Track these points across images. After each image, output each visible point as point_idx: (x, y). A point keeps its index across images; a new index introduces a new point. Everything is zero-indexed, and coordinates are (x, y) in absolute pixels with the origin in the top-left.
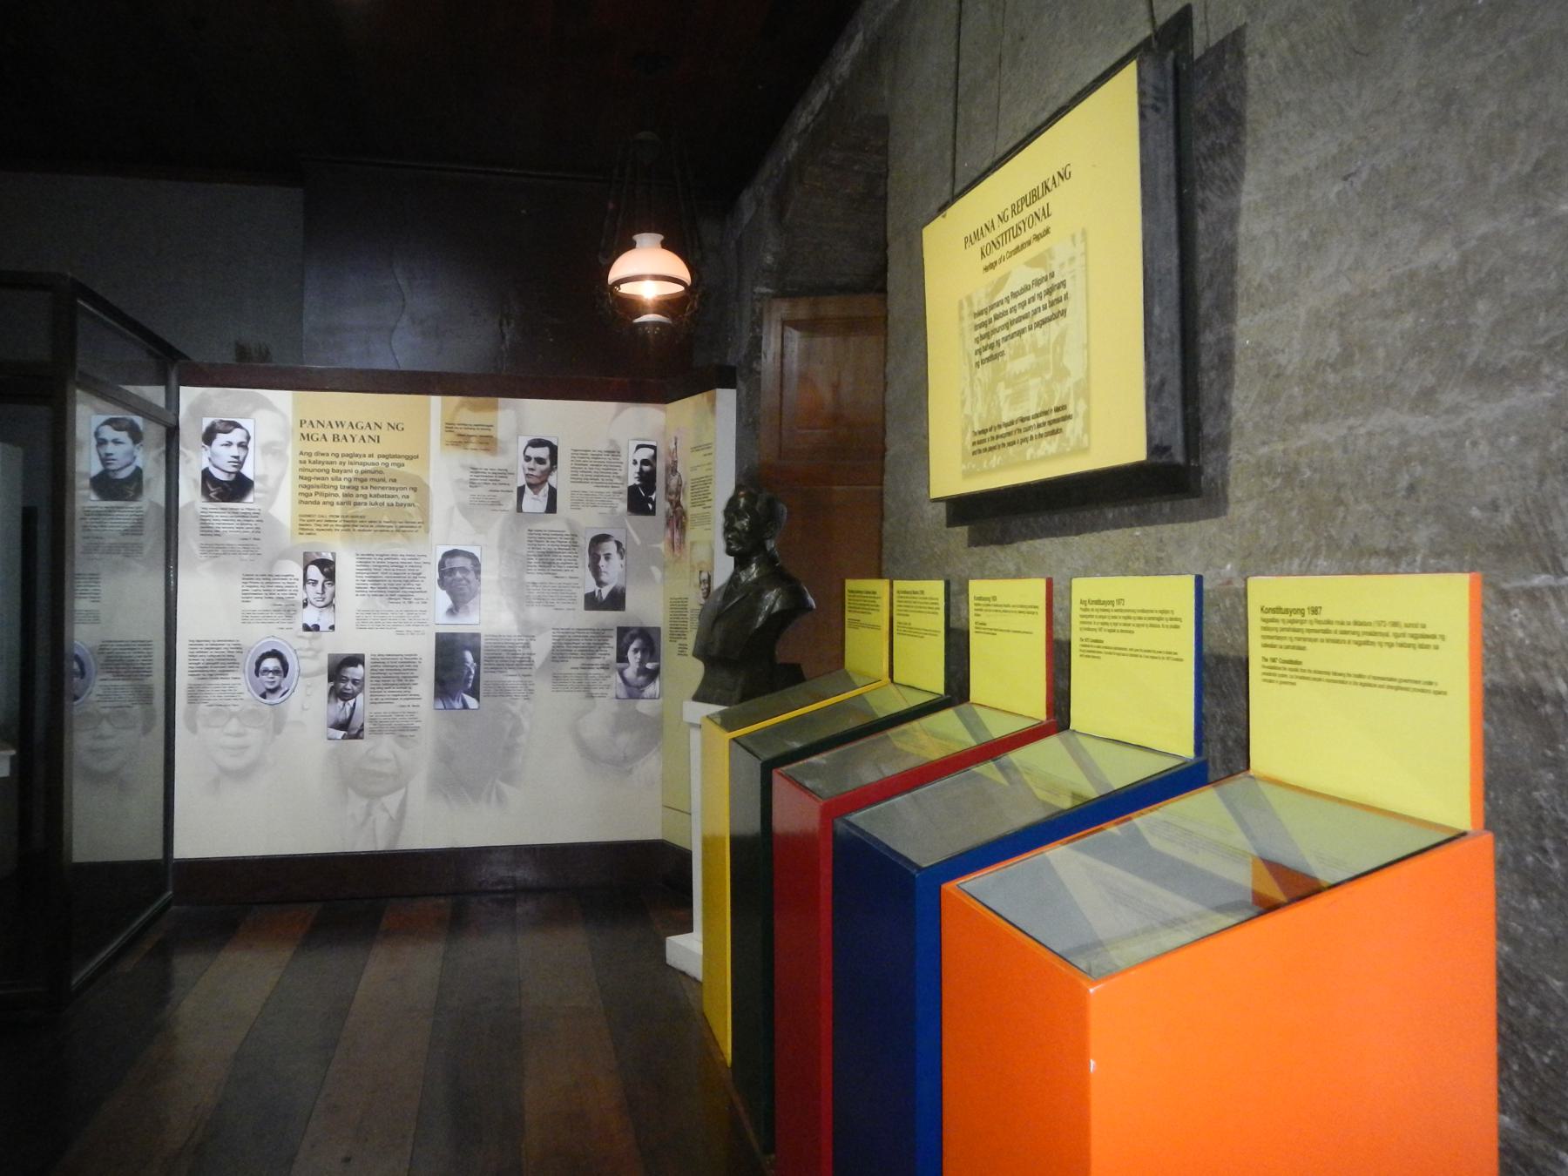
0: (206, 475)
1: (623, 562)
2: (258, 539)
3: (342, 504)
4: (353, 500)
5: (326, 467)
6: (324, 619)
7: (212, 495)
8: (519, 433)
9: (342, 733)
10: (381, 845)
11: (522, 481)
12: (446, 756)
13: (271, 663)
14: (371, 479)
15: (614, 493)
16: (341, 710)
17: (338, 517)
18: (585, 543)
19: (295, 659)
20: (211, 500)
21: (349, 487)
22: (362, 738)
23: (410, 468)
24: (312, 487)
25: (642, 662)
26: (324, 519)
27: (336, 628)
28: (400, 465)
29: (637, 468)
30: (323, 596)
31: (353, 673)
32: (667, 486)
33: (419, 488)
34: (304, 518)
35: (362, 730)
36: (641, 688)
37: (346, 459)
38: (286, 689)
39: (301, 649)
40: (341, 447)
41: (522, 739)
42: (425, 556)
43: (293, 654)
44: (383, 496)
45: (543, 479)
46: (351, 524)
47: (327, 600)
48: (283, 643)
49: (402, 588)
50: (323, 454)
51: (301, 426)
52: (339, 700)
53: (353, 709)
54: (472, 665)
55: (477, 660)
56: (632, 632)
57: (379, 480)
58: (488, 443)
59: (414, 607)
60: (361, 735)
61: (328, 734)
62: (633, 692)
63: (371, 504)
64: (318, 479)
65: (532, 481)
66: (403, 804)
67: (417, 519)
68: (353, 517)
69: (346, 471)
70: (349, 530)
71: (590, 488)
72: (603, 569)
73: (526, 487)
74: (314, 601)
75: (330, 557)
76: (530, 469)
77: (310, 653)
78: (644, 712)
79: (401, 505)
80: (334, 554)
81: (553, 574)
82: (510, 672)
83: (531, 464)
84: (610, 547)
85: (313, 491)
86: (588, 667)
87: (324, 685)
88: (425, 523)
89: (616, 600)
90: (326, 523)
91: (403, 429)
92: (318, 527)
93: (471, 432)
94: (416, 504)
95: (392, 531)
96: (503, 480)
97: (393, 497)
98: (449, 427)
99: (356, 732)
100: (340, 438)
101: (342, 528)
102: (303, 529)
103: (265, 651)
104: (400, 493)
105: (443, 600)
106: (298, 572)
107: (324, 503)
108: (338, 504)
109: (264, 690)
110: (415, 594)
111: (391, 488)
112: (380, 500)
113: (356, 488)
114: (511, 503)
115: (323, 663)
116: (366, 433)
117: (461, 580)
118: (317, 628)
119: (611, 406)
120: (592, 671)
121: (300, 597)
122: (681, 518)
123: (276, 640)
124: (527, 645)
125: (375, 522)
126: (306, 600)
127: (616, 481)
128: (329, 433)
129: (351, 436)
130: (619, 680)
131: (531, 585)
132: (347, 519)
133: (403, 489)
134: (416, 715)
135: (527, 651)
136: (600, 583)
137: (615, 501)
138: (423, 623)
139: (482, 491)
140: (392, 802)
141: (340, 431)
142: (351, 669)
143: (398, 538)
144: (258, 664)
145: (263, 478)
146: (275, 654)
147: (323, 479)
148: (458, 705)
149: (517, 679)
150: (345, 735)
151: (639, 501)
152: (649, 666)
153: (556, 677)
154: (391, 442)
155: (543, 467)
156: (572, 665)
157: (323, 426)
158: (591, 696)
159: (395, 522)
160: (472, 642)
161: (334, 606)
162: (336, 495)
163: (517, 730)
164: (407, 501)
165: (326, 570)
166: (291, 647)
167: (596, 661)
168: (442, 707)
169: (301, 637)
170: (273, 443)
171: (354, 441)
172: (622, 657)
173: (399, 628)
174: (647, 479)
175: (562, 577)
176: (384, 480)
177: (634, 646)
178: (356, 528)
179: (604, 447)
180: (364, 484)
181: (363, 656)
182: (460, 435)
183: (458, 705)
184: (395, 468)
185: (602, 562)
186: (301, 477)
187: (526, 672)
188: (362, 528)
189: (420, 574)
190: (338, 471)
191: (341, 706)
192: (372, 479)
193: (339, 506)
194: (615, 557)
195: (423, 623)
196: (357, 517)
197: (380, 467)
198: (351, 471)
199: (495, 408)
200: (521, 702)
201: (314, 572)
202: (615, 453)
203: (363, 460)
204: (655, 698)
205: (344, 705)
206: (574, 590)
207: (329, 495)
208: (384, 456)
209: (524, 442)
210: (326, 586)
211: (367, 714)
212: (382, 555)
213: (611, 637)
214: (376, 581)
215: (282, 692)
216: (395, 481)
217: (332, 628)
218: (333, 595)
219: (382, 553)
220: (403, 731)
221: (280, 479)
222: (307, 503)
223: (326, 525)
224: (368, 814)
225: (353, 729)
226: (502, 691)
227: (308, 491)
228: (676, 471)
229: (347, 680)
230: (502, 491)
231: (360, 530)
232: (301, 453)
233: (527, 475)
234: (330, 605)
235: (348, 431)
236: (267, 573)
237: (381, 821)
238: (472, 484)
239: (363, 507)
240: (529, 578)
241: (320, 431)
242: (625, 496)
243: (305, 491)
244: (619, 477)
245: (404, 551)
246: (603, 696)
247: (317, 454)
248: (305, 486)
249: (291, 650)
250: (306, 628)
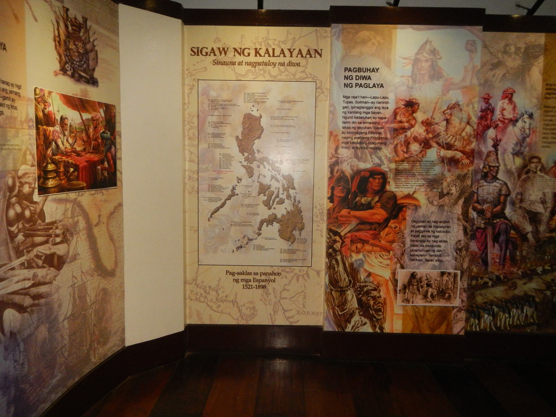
122: (507, 232)
228: (495, 178)
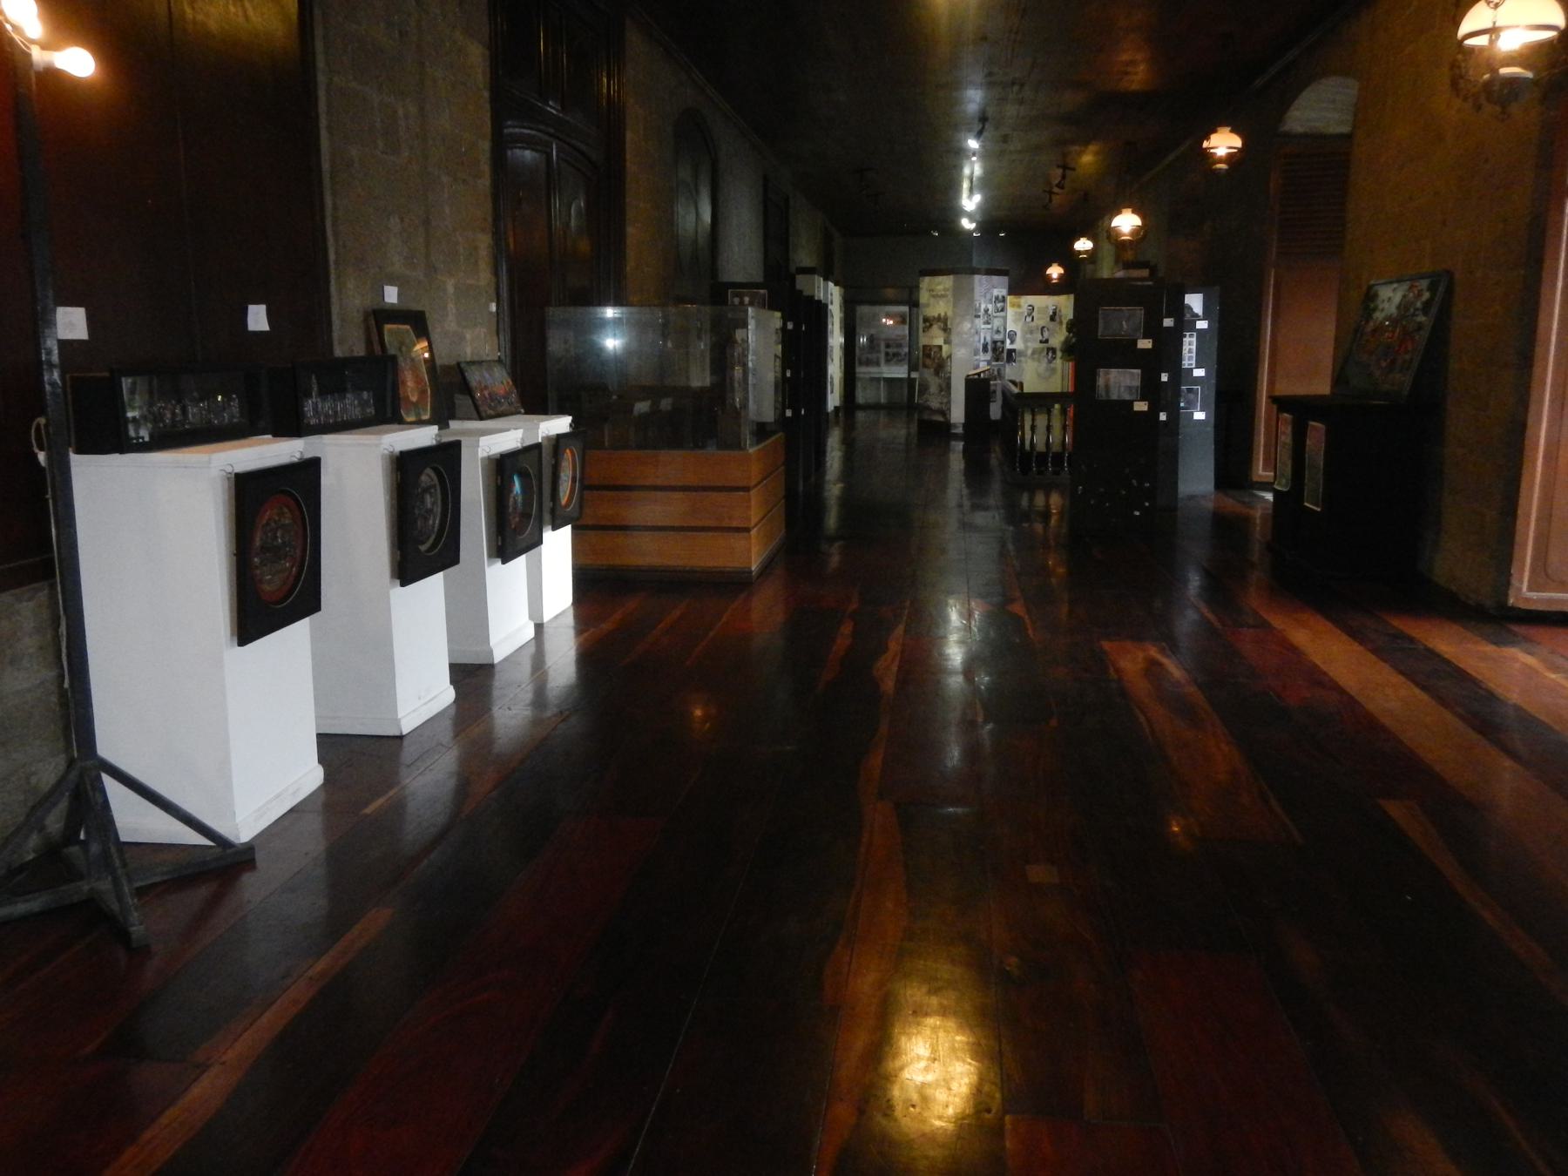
58: (1019, 306)
62: (1050, 362)
84: (1045, 329)
89: (1047, 341)
119: (1046, 297)
151: (1052, 318)
156: (1036, 356)
160: (1014, 350)
172: (1047, 354)
174: (1055, 313)
202: (1047, 307)
226: (1020, 361)
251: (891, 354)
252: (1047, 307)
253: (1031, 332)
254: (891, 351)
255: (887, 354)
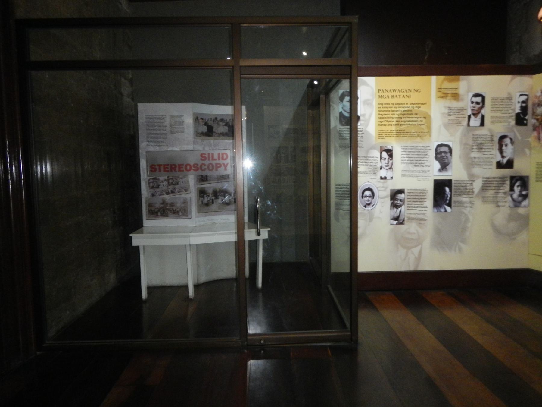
0: (341, 114)
1: (512, 147)
2: (362, 141)
3: (396, 125)
4: (400, 123)
5: (389, 109)
6: (388, 174)
7: (343, 123)
8: (469, 91)
9: (396, 222)
10: (411, 268)
11: (469, 112)
12: (438, 231)
13: (368, 193)
14: (408, 113)
15: (510, 116)
16: (395, 212)
17: (394, 131)
18: (496, 139)
19: (377, 191)
20: (343, 125)
21: (398, 118)
22: (404, 224)
23: (423, 108)
24: (383, 118)
25: (521, 191)
26: (388, 132)
27: (393, 178)
28: (419, 107)
29: (519, 105)
30: (388, 164)
31: (400, 197)
32: (534, 113)
33: (427, 117)
34: (380, 132)
35: (404, 221)
36: (520, 202)
37: (397, 106)
38: (374, 204)
39: (379, 187)
40: (395, 101)
41: (469, 225)
42: (429, 146)
43: (376, 189)
44: (412, 121)
45: (479, 111)
46: (400, 134)
47: (390, 167)
48: (373, 185)
49: (420, 161)
50: (388, 104)
51: (379, 92)
52: (395, 208)
53: (400, 212)
54: (448, 193)
55: (451, 191)
56: (516, 178)
57: (410, 114)
58: (456, 96)
59: (425, 168)
60: (403, 223)
61: (390, 222)
62: (517, 204)
63: (407, 125)
64: (386, 115)
65: (475, 112)
66: (420, 253)
67: (426, 130)
68: (400, 130)
69: (397, 111)
70: (398, 136)
71: (499, 114)
72: (504, 151)
73: (472, 116)
74: (384, 167)
75: (391, 148)
76: (474, 107)
77: (383, 189)
78: (521, 213)
79: (419, 125)
80: (392, 147)
81: (483, 153)
82: (464, 196)
83: (474, 105)
84: (507, 141)
85: (383, 120)
86: (497, 193)
87: (388, 202)
88: (429, 133)
89: (510, 164)
90: (389, 133)
91: (420, 92)
92: (386, 135)
93: (448, 92)
94: (426, 124)
95: (416, 136)
96: (462, 113)
97: (416, 121)
98: (439, 90)
99: (401, 221)
100: (395, 96)
101: (395, 135)
102: (380, 136)
103: (365, 188)
104: (419, 120)
105: (437, 165)
106: (377, 154)
107: (388, 125)
108: (394, 125)
109: (365, 204)
110: (425, 163)
111: (415, 118)
112: (411, 123)
113: (401, 118)
114: (465, 122)
115: (388, 193)
116: (405, 94)
117: (444, 156)
118: (385, 178)
119: (508, 77)
120: (499, 195)
121: (379, 165)
123: (370, 183)
124: (471, 184)
125: (409, 132)
126: (381, 166)
127: (511, 111)
128: (390, 94)
129: (399, 95)
130: (510, 199)
131: (473, 158)
132: (397, 131)
133: (421, 118)
134: (426, 215)
135: (471, 187)
136: (503, 157)
137: (510, 120)
138: (428, 175)
139: (453, 117)
140: (416, 250)
141: (394, 94)
142: (399, 195)
143: (418, 139)
144: (363, 193)
145: (364, 115)
146: (369, 189)
147: (388, 114)
148: (443, 210)
149: (467, 199)
150: (397, 223)
151: (520, 120)
152: (524, 193)
153: (484, 198)
154: (415, 98)
155: (479, 106)
156: (490, 193)
157: (387, 92)
158: (498, 206)
159: (417, 132)
160: (448, 183)
161: (392, 168)
162: (393, 121)
163: (467, 220)
164: (422, 123)
165: (389, 153)
166: (375, 186)
167: (501, 191)
168: (436, 211)
169: (379, 182)
170: (368, 100)
171: (400, 98)
172: (512, 189)
173: (419, 178)
174: (524, 109)
175: (486, 155)
176: (412, 114)
177: (517, 184)
178: (401, 135)
179: (505, 95)
180: (405, 116)
181: (404, 190)
182: (444, 93)
183: (443, 210)
184: (417, 109)
185: (504, 148)
186: (379, 114)
187: (471, 196)
188: (403, 135)
189: (427, 154)
190: (393, 111)
191: (396, 211)
192: (408, 114)
193: (394, 126)
194: (510, 145)
195: (428, 175)
196: (401, 130)
197: (411, 109)
198: (399, 111)
199: (458, 80)
200: (468, 209)
201: (385, 154)
202: (510, 98)
203: (404, 106)
204: (526, 207)
205: (397, 210)
206: (491, 160)
207: (390, 121)
208: (412, 104)
209: (471, 95)
210: (389, 160)
211: (406, 214)
212: (412, 147)
213: (507, 180)
214: (409, 157)
215: (372, 205)
216: (417, 114)
217: (392, 178)
218: (392, 164)
219: (412, 146)
220: (420, 221)
221: (370, 115)
222: (381, 125)
223: (389, 134)
224: (407, 255)
225: (401, 220)
226: (461, 204)
227: (382, 119)
229: (398, 200)
230: (461, 117)
231: (403, 136)
232: (379, 104)
233: (472, 110)
234: (391, 168)
235: (397, 93)
236: (365, 155)
237: (412, 258)
238: (449, 115)
239: (403, 127)
240: (473, 155)
241: (386, 94)
242: (514, 118)
243: (380, 120)
244: (512, 109)
245: (420, 145)
246: (504, 206)
247: (385, 104)
248: (381, 118)
249: (375, 188)
250: (381, 178)
251: (210, 191)
252: (510, 98)
253: (480, 148)
254: (207, 186)
255: (202, 193)
